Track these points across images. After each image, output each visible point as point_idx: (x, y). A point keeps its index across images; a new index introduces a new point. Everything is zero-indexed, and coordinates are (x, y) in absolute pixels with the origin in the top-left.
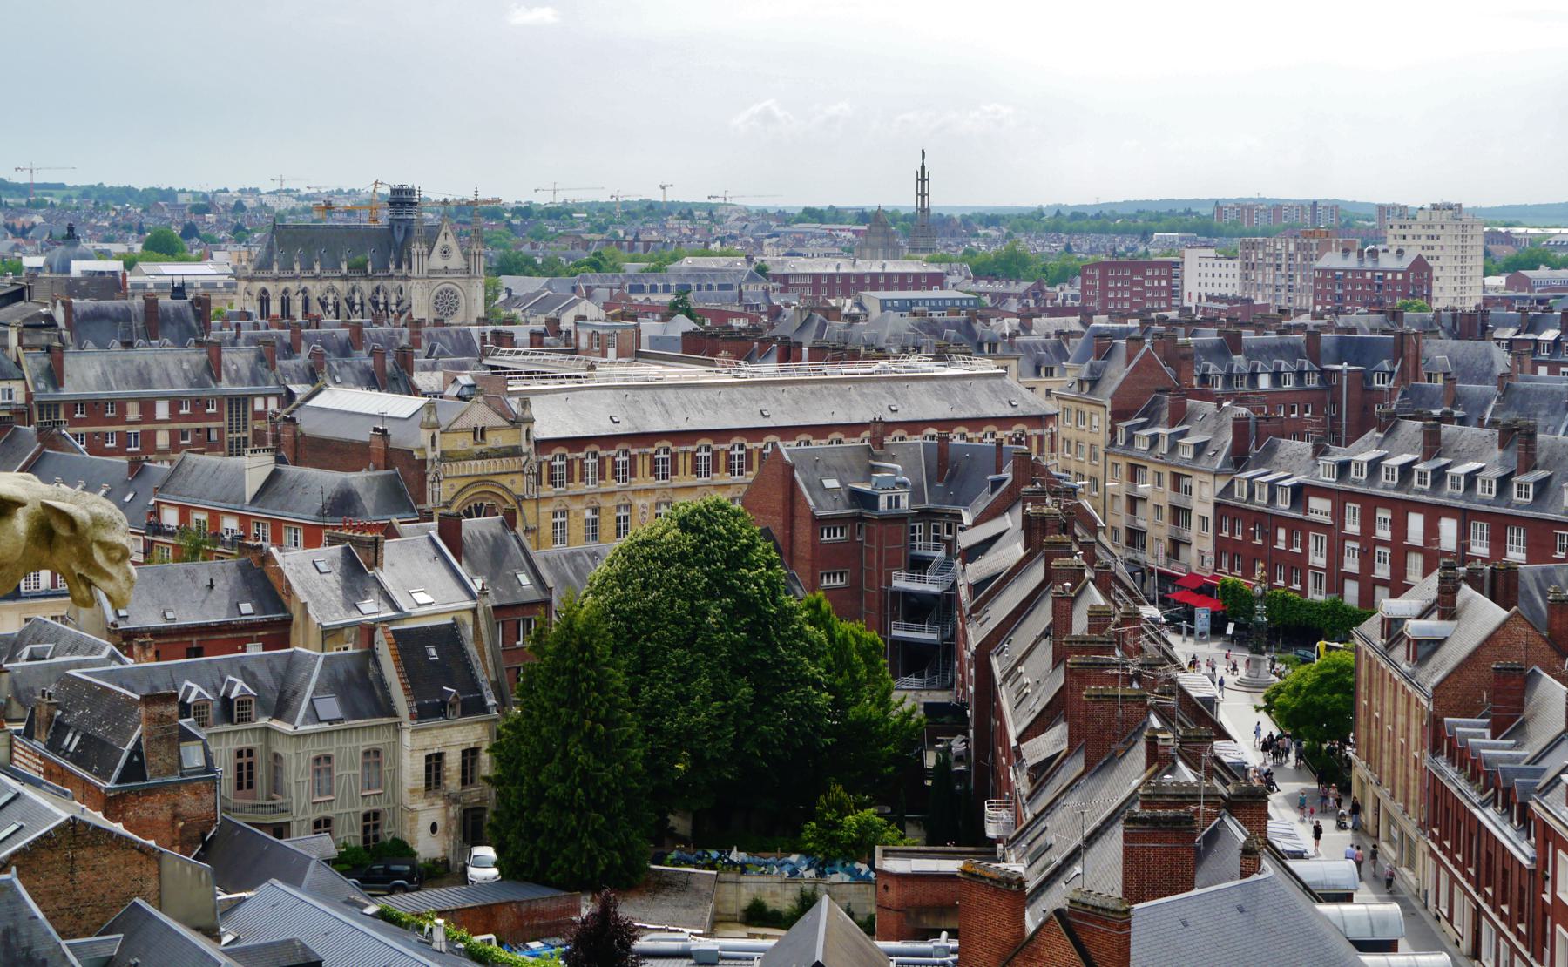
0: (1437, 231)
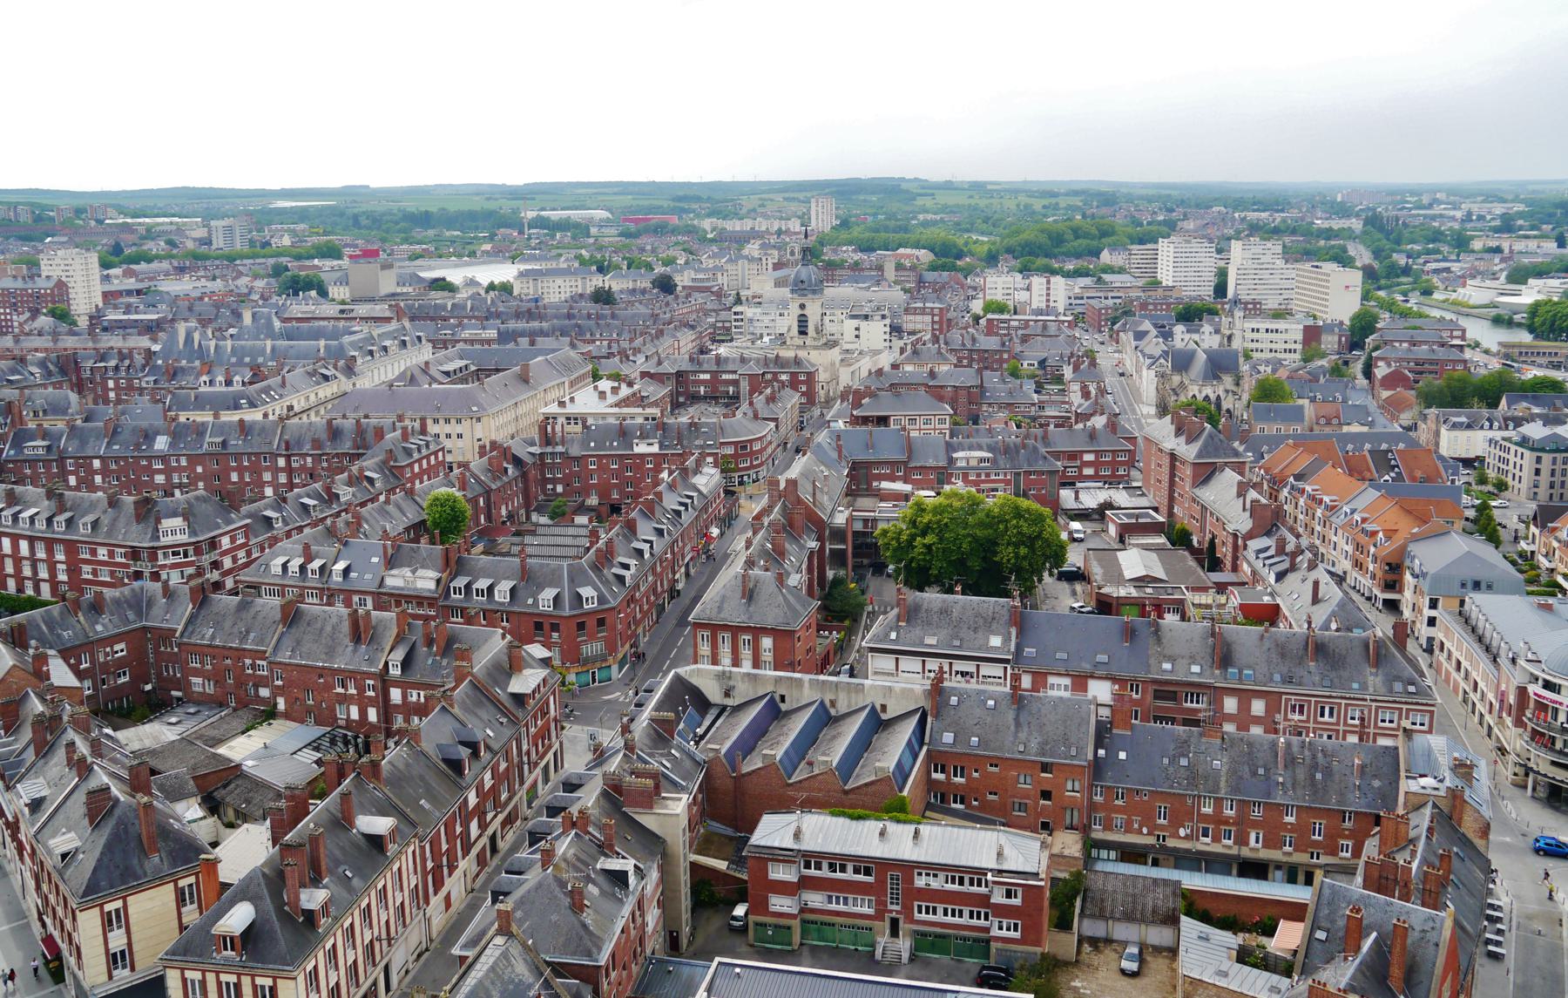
0: (70, 261)
